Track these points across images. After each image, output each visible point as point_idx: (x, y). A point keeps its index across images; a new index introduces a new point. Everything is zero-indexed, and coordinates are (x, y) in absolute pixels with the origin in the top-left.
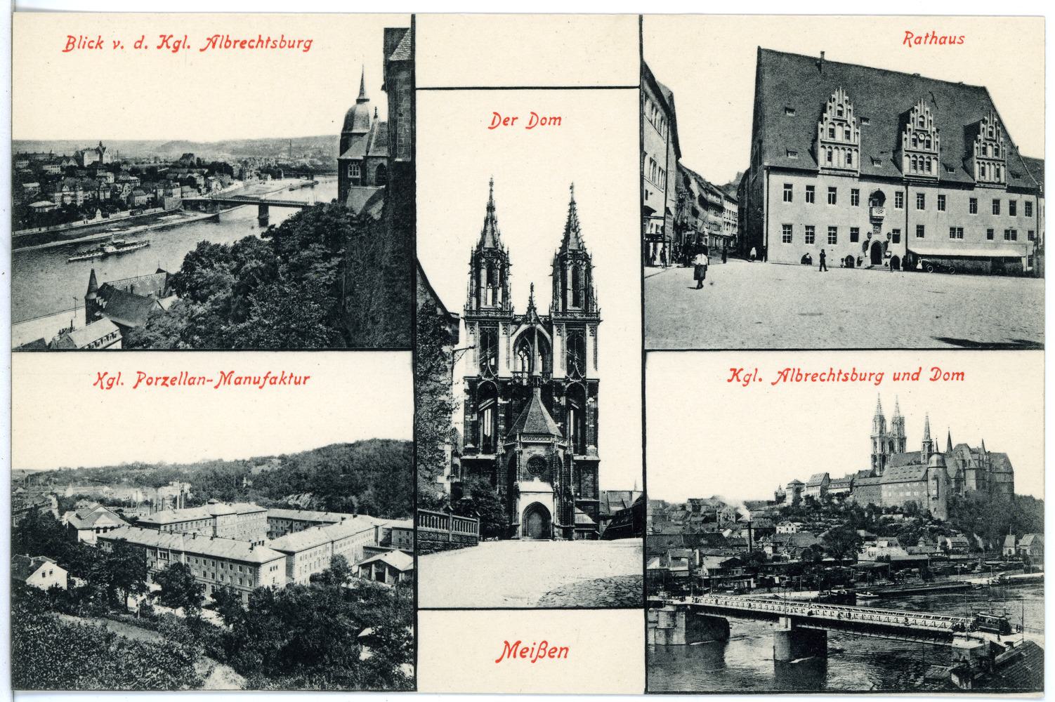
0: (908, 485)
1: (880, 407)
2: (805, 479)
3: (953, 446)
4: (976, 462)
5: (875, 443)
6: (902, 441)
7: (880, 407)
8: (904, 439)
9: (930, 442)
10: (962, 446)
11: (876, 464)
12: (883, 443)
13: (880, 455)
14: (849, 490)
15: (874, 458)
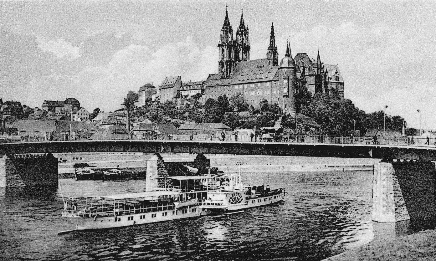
0: (259, 85)
1: (227, 18)
2: (157, 83)
3: (294, 56)
4: (316, 69)
5: (223, 51)
6: (247, 49)
7: (227, 18)
8: (249, 48)
9: (276, 49)
10: (302, 56)
11: (223, 70)
12: (230, 51)
13: (227, 61)
14: (200, 91)
15: (221, 64)
